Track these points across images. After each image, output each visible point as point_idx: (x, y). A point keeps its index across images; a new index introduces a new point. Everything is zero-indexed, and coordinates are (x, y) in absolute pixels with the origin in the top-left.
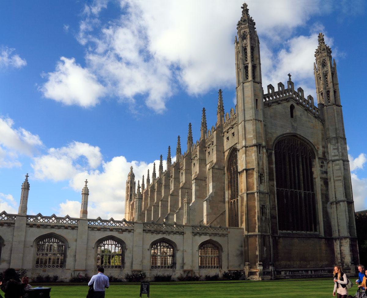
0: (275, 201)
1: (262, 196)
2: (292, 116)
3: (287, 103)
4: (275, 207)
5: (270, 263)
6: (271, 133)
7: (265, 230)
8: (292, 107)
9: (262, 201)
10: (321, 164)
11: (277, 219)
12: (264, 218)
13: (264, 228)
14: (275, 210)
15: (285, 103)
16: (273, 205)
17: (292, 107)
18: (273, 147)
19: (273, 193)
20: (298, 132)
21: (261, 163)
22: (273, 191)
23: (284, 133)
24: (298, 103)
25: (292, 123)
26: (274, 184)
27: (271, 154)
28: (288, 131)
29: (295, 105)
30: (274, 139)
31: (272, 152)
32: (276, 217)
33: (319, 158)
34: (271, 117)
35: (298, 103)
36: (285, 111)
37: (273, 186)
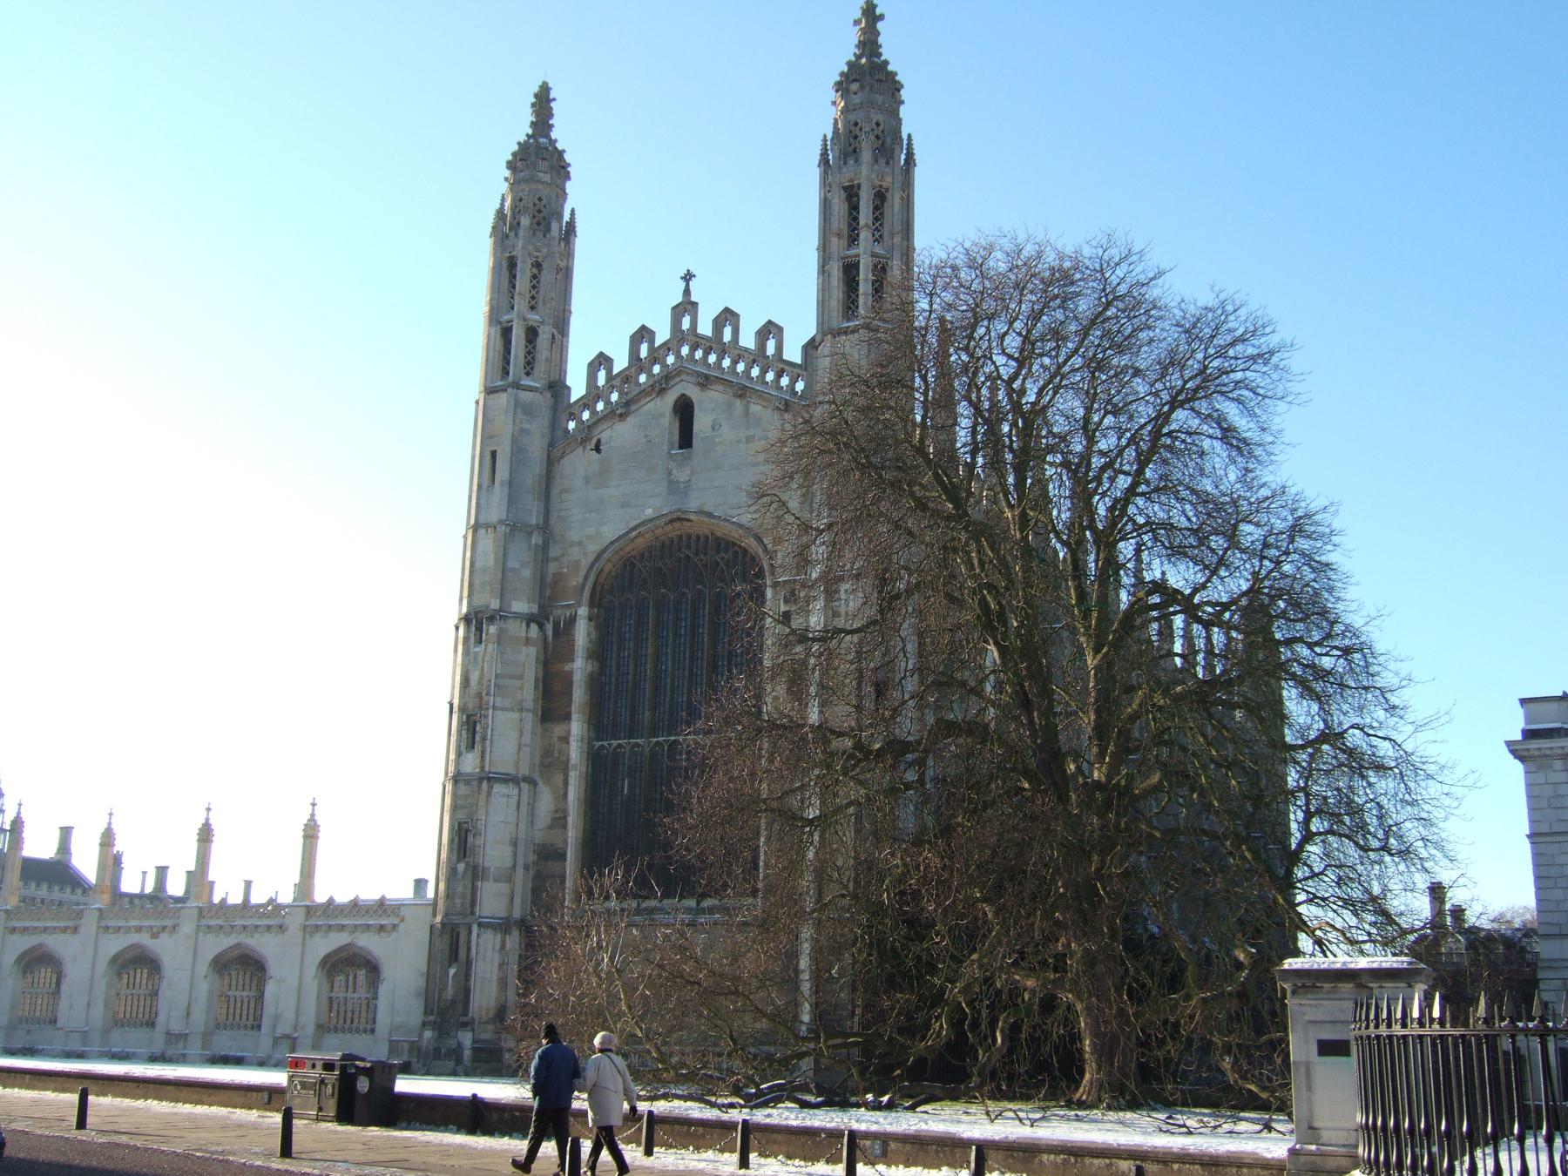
0: (565, 796)
1: (463, 789)
2: (686, 440)
3: (659, 399)
4: (565, 818)
5: (465, 1019)
6: (580, 543)
7: (462, 906)
8: (684, 410)
9: (462, 807)
10: (783, 608)
11: (565, 860)
12: (461, 867)
13: (458, 901)
14: (565, 827)
15: (652, 404)
16: (556, 811)
17: (684, 410)
18: (581, 596)
19: (563, 766)
20: (693, 504)
21: (475, 677)
22: (563, 758)
23: (632, 525)
24: (705, 381)
25: (670, 474)
26: (569, 732)
27: (572, 621)
28: (649, 512)
29: (693, 393)
30: (585, 563)
31: (576, 615)
32: (565, 854)
33: (775, 585)
34: (587, 480)
35: (705, 381)
36: (646, 436)
37: (565, 739)
